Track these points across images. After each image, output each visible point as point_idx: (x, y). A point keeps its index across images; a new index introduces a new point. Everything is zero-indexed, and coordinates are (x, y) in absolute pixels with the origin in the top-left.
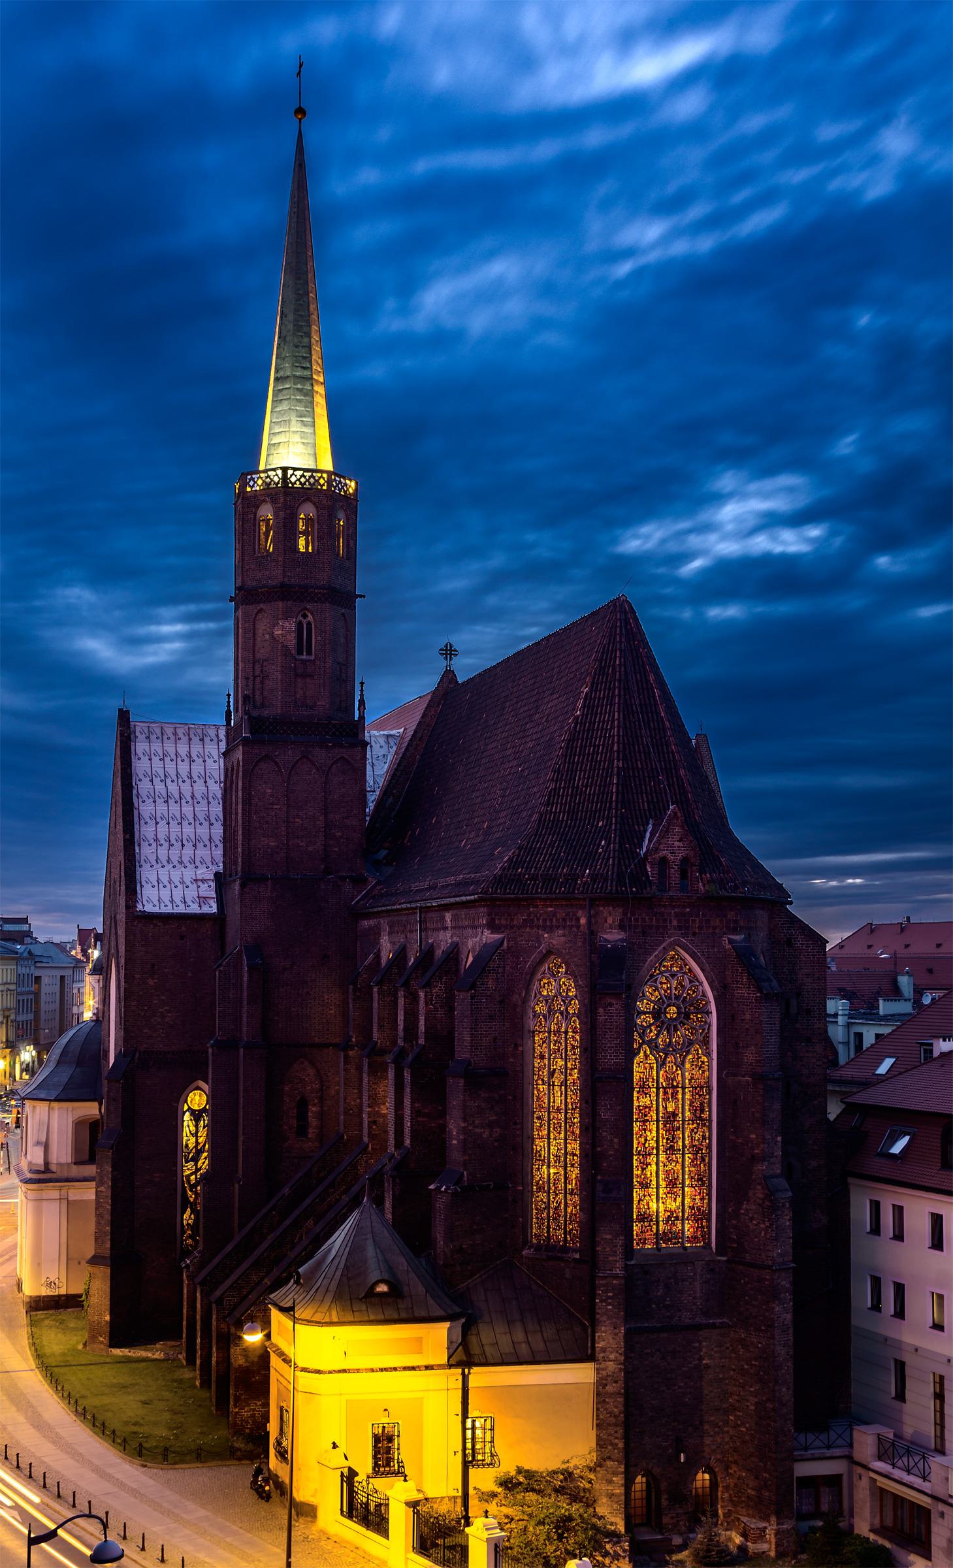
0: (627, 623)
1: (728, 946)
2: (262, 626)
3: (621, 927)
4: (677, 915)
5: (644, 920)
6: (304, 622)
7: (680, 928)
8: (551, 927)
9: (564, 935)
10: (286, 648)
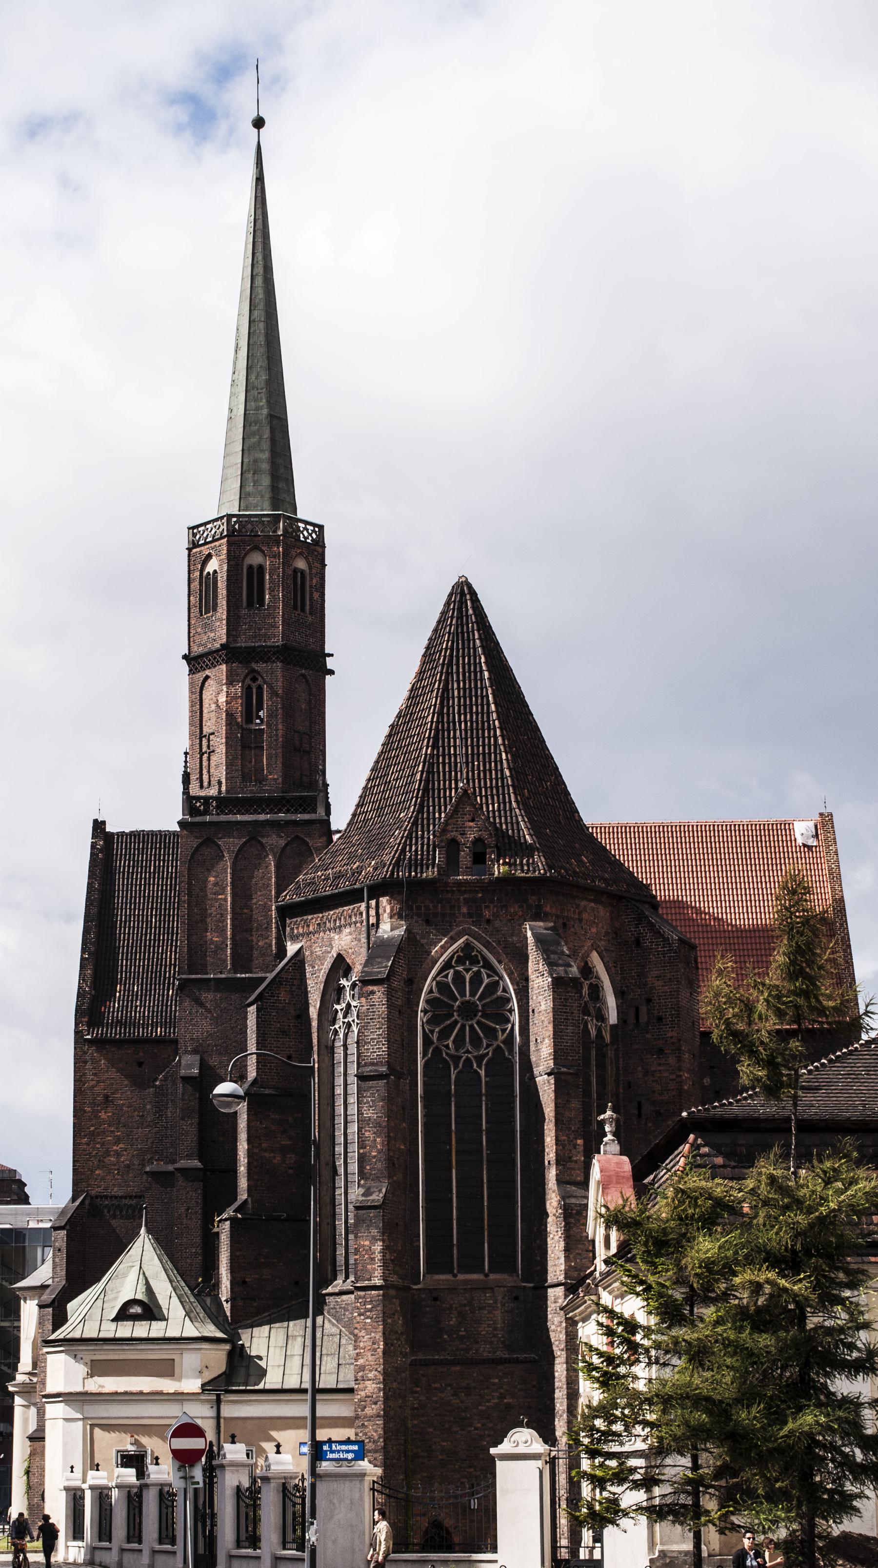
5: (427, 908)
7: (470, 915)
8: (340, 927)
9: (350, 933)
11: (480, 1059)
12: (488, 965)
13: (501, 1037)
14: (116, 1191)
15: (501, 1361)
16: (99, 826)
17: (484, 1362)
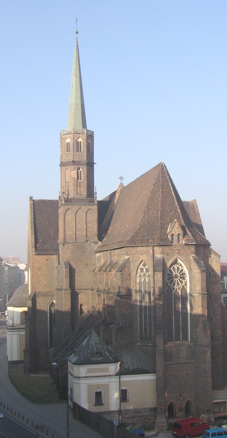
0: (163, 169)
1: (192, 258)
2: (68, 172)
3: (162, 253)
4: (177, 250)
6: (79, 171)
10: (74, 178)
11: (179, 288)
12: (181, 265)
13: (184, 283)
14: (43, 291)
15: (185, 363)
16: (31, 198)
17: (183, 363)
